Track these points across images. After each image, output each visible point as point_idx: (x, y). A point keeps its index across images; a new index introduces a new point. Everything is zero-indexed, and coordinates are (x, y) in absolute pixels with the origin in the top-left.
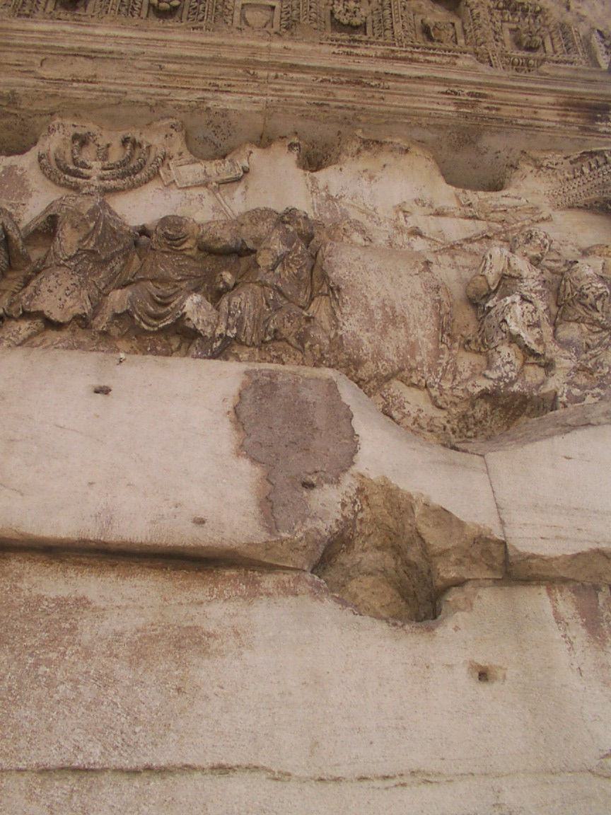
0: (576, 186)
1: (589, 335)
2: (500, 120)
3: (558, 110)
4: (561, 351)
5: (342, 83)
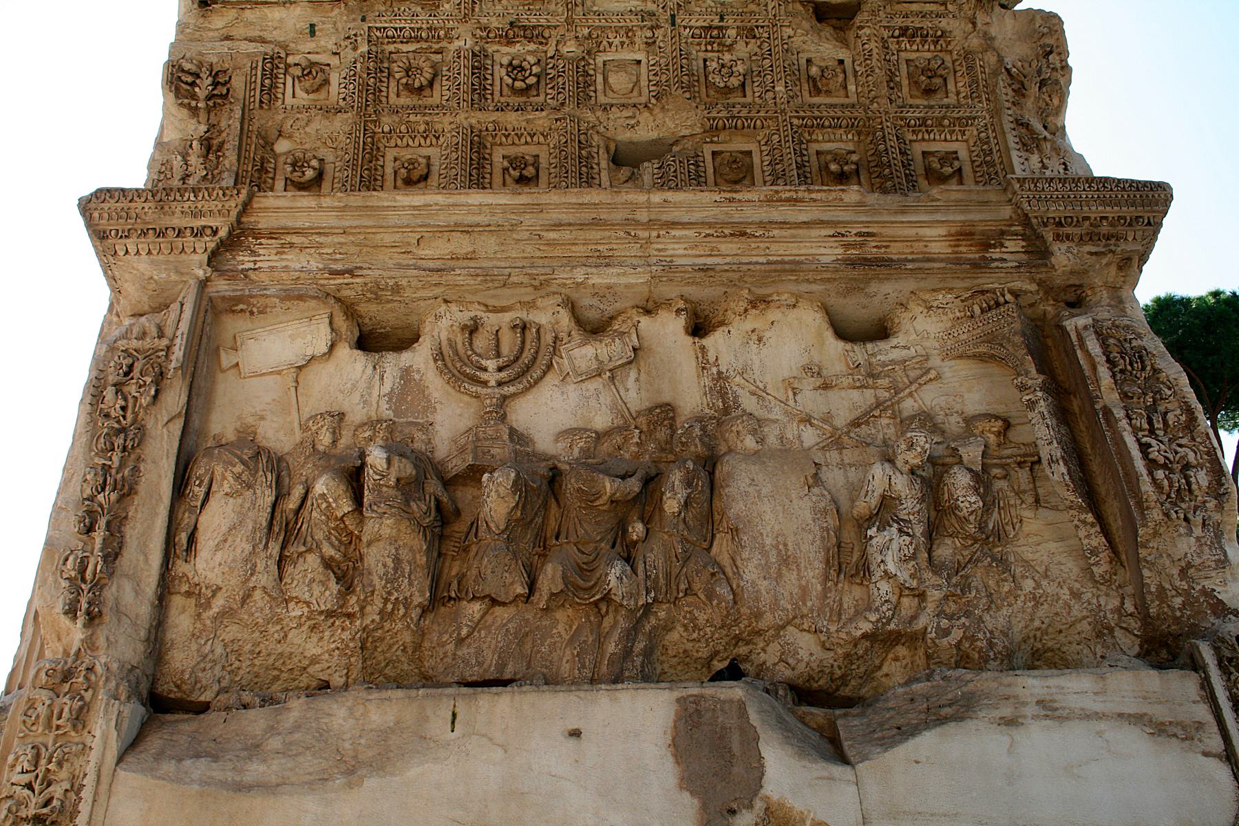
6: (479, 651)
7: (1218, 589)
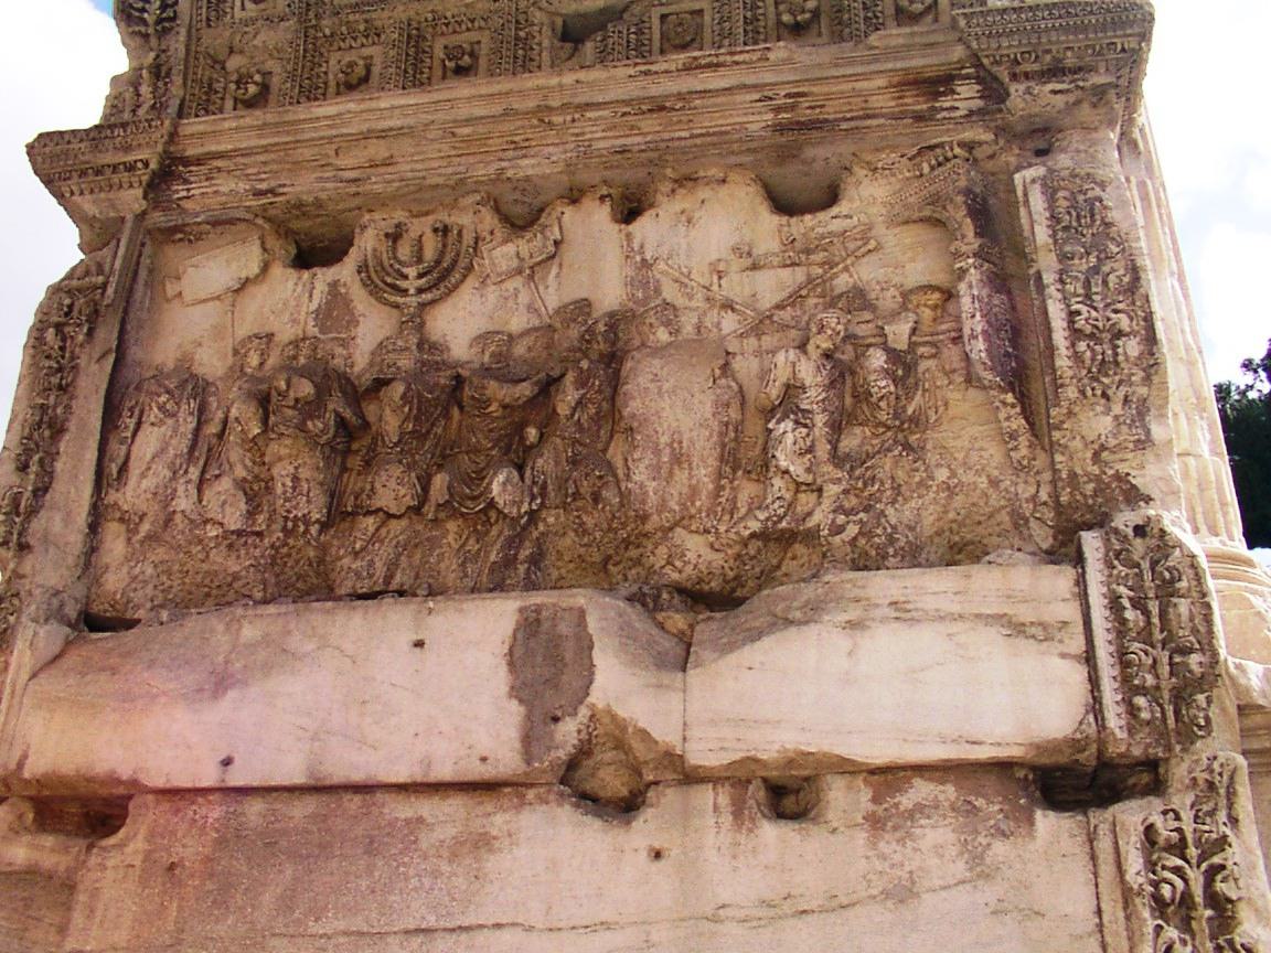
5: (644, 113)
6: (371, 563)
7: (1133, 473)
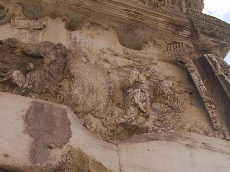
0: (168, 53)
1: (163, 108)
2: (144, 24)
3: (166, 24)
4: (152, 112)
